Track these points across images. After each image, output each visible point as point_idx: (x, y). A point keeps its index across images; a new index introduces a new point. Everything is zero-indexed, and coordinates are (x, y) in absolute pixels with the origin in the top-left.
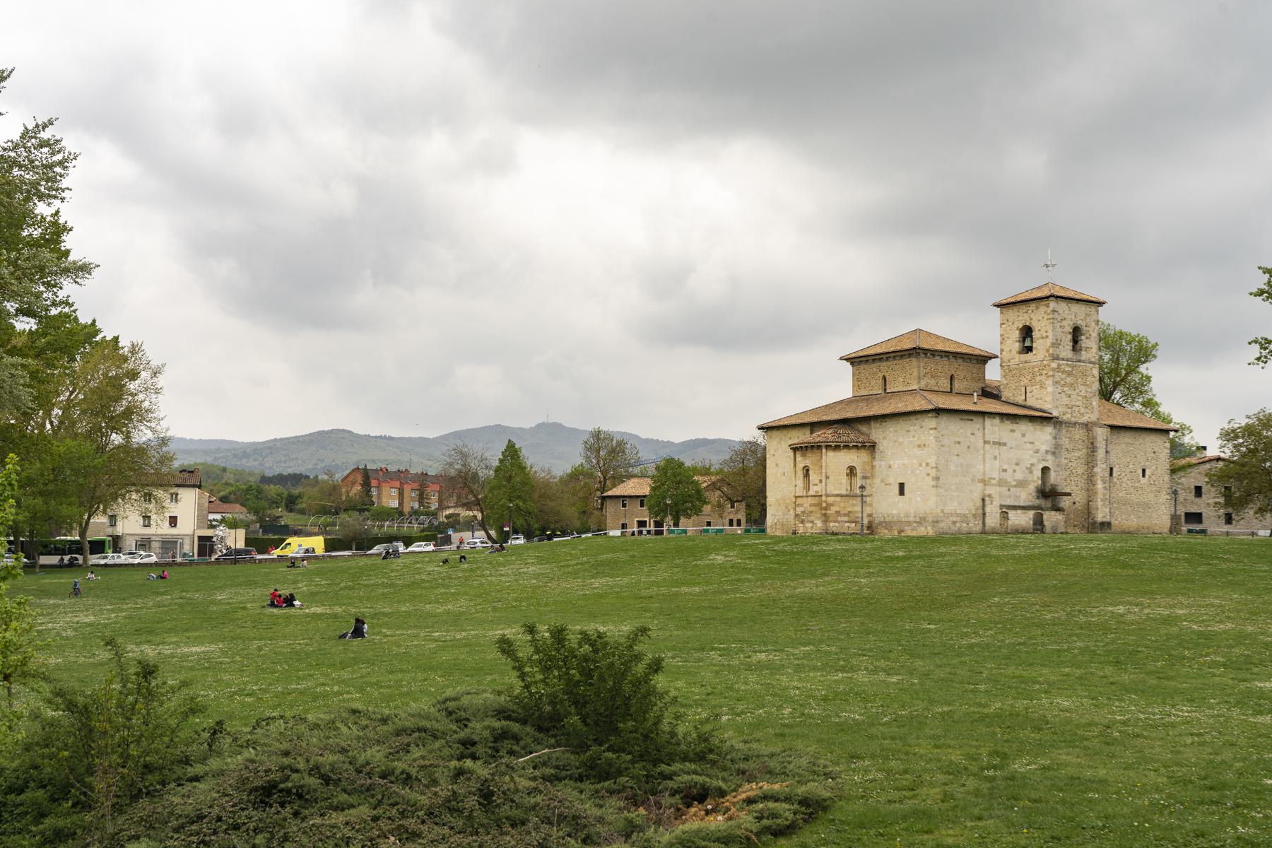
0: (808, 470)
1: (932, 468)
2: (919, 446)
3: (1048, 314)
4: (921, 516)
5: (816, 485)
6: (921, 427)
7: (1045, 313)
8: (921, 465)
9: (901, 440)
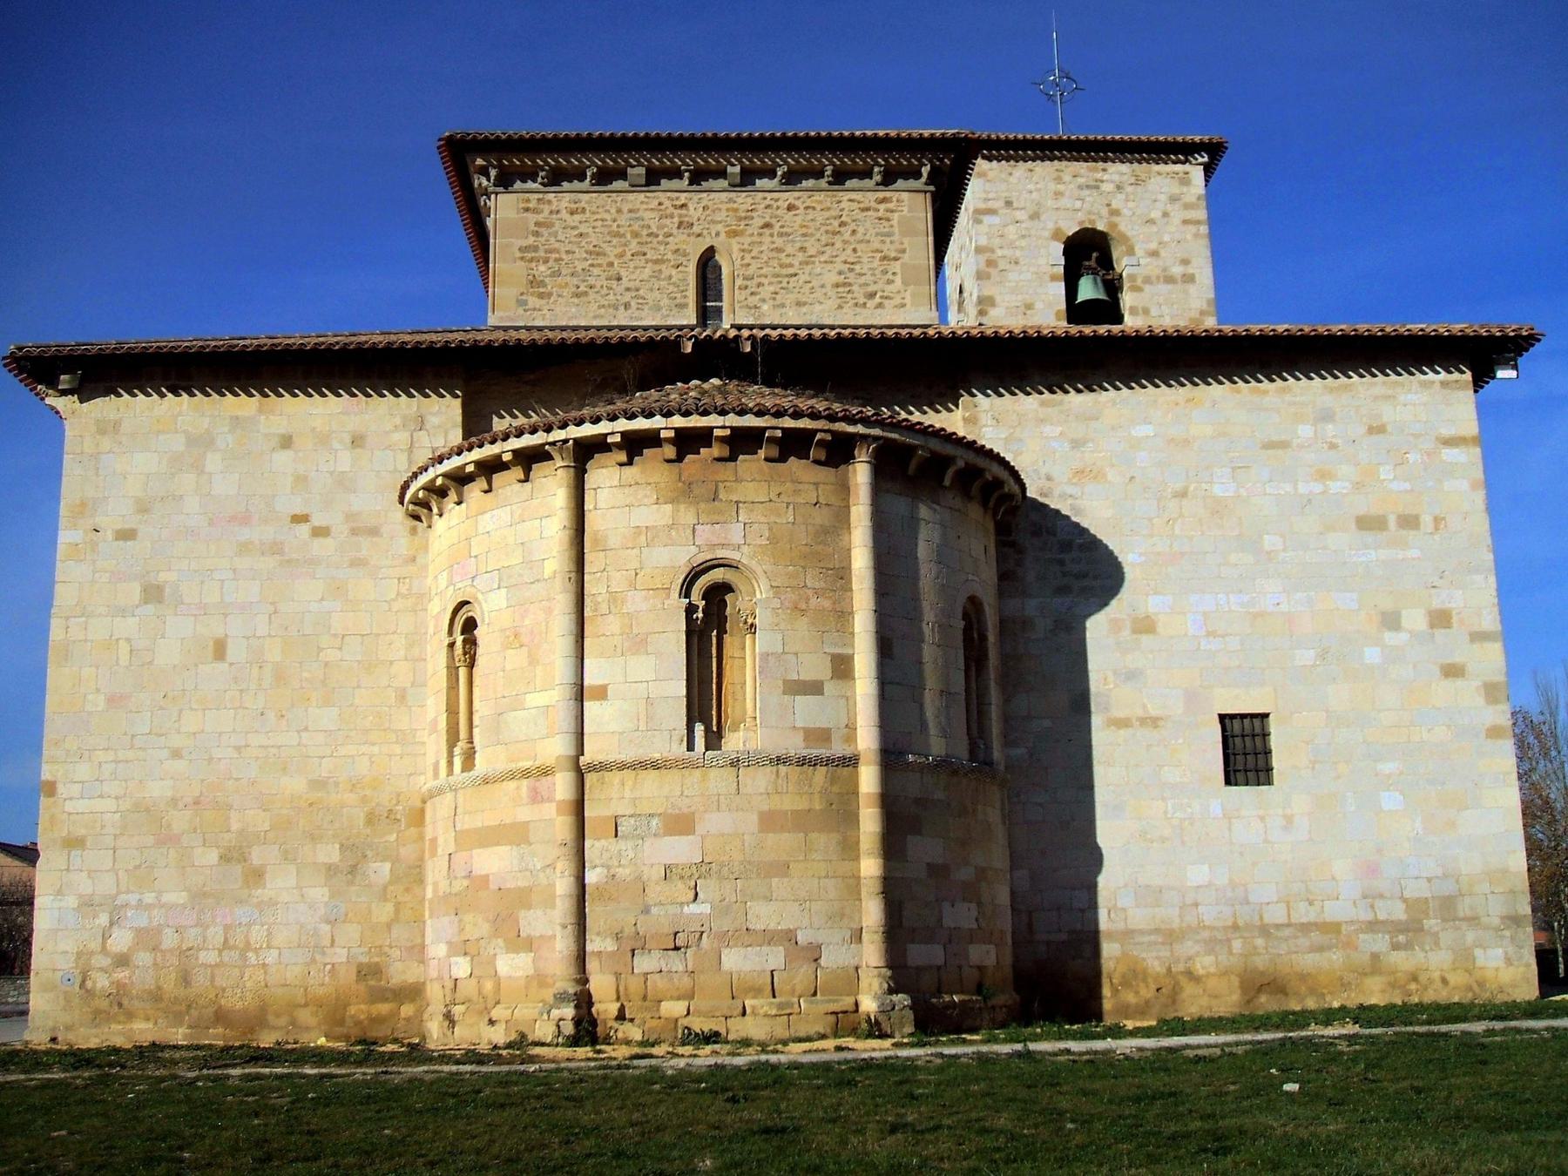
0: (718, 594)
1: (1478, 637)
2: (1369, 523)
3: (1187, 206)
4: (1416, 890)
5: (815, 688)
6: (1377, 430)
7: (1174, 199)
8: (1391, 621)
9: (1221, 489)
